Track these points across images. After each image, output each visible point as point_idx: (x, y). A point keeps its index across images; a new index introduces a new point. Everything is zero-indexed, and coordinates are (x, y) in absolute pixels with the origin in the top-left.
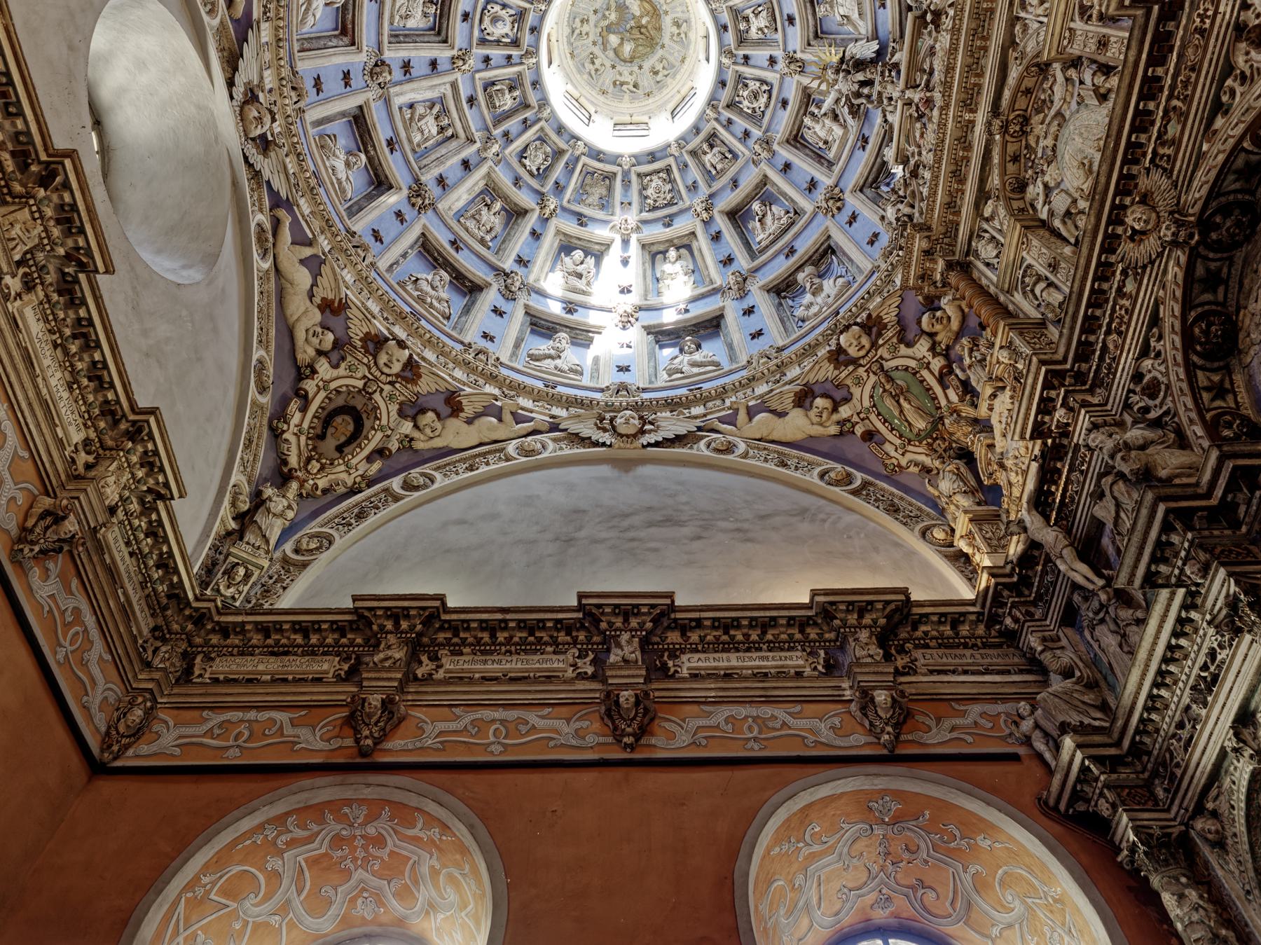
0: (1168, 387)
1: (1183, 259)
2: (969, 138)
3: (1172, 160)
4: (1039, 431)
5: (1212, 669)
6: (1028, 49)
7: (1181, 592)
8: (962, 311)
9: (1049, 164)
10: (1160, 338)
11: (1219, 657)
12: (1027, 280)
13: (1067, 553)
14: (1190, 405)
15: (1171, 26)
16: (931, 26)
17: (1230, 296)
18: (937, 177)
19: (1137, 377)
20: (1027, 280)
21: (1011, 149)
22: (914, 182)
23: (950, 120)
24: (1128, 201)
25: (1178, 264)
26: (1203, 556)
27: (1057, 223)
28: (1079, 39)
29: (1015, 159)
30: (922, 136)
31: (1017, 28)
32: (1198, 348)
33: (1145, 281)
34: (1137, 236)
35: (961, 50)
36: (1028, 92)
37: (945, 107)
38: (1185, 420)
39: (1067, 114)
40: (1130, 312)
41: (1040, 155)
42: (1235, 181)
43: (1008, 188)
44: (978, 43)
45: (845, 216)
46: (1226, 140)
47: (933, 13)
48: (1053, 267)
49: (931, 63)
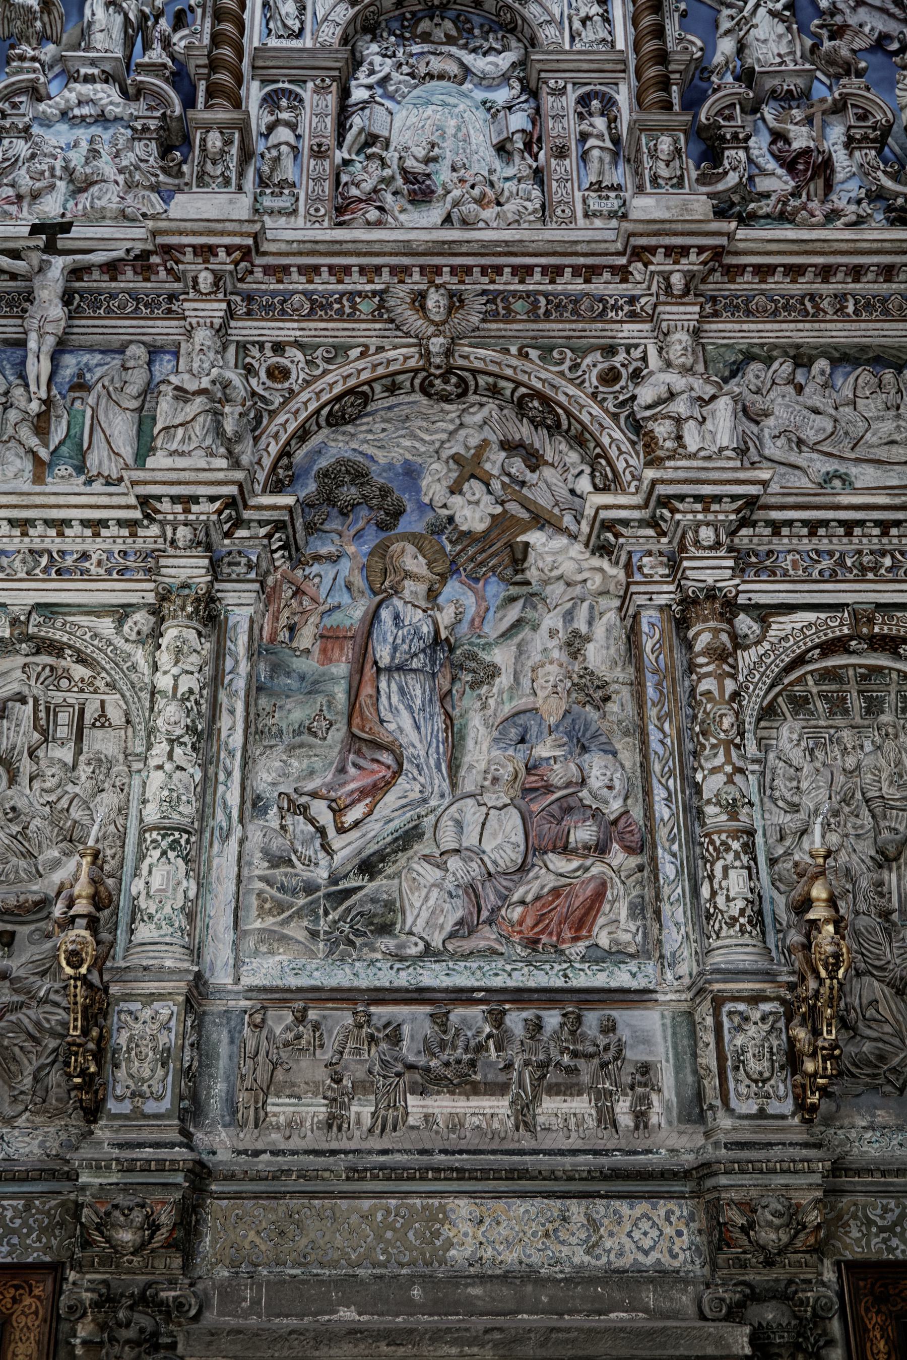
1: (412, 363)
4: (166, 250)
5: (69, 561)
7: (137, 514)
9: (412, 75)
10: (328, 361)
11: (87, 564)
13: (50, 341)
19: (278, 348)
20: (284, 103)
24: (446, 277)
26: (202, 536)
27: (357, 121)
33: (378, 326)
34: (419, 300)
38: (273, 429)
39: (467, 86)
40: (341, 316)
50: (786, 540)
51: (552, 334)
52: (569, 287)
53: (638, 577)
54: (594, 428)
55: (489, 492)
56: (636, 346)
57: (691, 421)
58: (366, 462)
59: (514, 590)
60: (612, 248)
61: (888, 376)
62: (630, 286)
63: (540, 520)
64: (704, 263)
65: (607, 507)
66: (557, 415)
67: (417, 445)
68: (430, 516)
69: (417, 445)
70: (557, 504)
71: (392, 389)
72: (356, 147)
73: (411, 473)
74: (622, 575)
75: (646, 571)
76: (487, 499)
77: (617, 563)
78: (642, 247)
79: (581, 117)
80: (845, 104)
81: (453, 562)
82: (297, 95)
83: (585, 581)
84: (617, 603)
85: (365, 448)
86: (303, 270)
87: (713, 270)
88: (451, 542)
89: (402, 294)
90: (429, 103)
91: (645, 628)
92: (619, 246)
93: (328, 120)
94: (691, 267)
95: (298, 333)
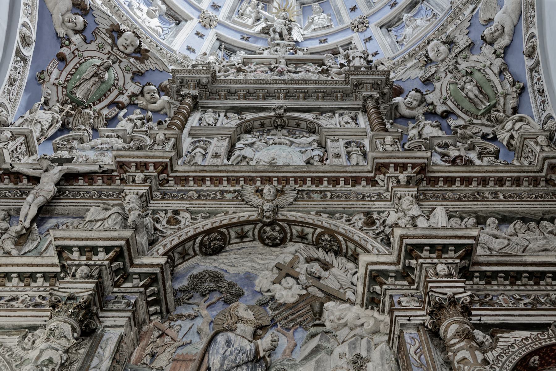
0: (179, 229)
1: (253, 218)
2: (270, 98)
3: (303, 199)
6: (322, 121)
8: (161, 110)
9: (266, 143)
10: (205, 218)
12: (202, 143)
14: (174, 243)
15: (364, 183)
16: (320, 69)
17: (234, 245)
18: (245, 83)
20: (202, 143)
21: (267, 122)
22: (234, 70)
23: (278, 86)
24: (275, 183)
25: (249, 216)
27: (237, 153)
28: (335, 144)
29: (262, 125)
30: (262, 72)
31: (330, 114)
32: (206, 238)
33: (235, 203)
34: (259, 192)
35: (316, 86)
36: (298, 125)
37: (285, 82)
40: (214, 199)
41: (268, 137)
42: (297, 231)
43: (247, 124)
44: (320, 95)
45: (202, 31)
46: (320, 221)
47: (327, 70)
48: (216, 155)
49: (301, 72)
50: (496, 287)
51: (334, 206)
52: (343, 189)
53: (398, 307)
54: (363, 243)
55: (298, 283)
56: (383, 212)
57: (421, 217)
58: (222, 272)
59: (313, 330)
60: (366, 169)
61: (532, 225)
62: (377, 188)
63: (330, 296)
64: (418, 173)
65: (373, 264)
66: (339, 242)
67: (254, 265)
68: (260, 297)
69: (254, 265)
70: (342, 288)
71: (242, 236)
72: (236, 162)
73: (249, 278)
74: (387, 319)
75: (403, 304)
76: (296, 287)
77: (383, 311)
78: (381, 163)
79: (346, 147)
80: (474, 146)
81: (272, 320)
82: (209, 142)
83: (362, 325)
84: (387, 338)
85: (222, 266)
86: (195, 180)
87: (422, 180)
88: (271, 309)
89: (250, 189)
90: (272, 149)
91: (408, 340)
92: (369, 168)
93: (223, 149)
94: (409, 174)
95: (189, 206)
